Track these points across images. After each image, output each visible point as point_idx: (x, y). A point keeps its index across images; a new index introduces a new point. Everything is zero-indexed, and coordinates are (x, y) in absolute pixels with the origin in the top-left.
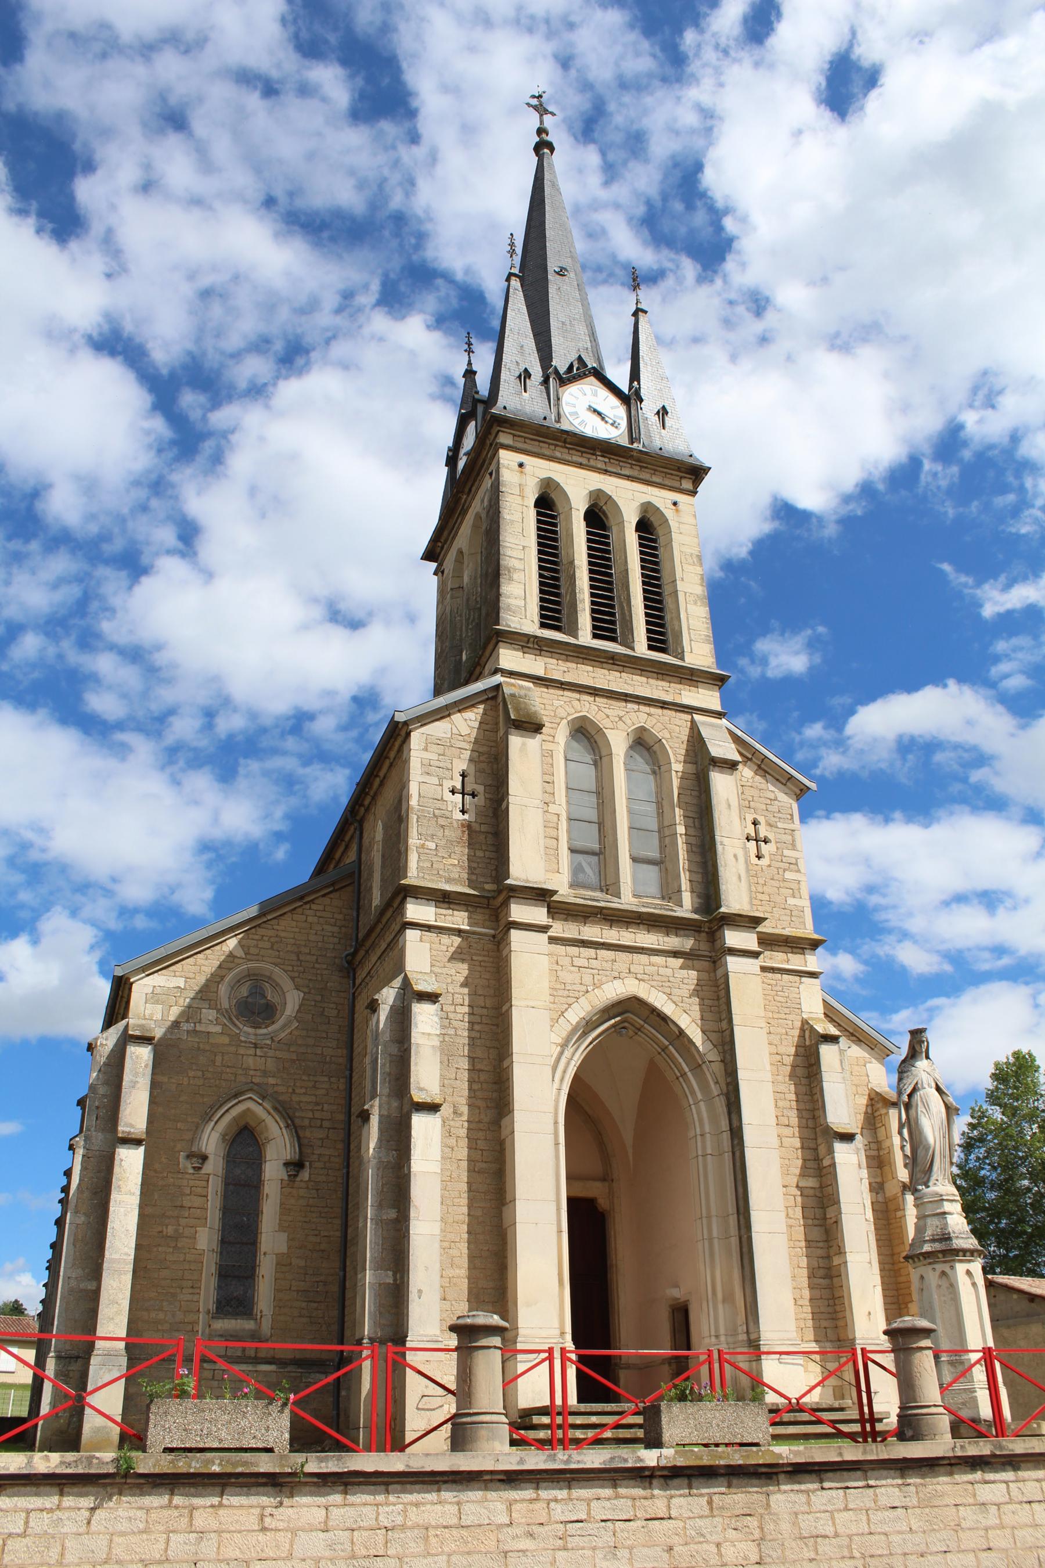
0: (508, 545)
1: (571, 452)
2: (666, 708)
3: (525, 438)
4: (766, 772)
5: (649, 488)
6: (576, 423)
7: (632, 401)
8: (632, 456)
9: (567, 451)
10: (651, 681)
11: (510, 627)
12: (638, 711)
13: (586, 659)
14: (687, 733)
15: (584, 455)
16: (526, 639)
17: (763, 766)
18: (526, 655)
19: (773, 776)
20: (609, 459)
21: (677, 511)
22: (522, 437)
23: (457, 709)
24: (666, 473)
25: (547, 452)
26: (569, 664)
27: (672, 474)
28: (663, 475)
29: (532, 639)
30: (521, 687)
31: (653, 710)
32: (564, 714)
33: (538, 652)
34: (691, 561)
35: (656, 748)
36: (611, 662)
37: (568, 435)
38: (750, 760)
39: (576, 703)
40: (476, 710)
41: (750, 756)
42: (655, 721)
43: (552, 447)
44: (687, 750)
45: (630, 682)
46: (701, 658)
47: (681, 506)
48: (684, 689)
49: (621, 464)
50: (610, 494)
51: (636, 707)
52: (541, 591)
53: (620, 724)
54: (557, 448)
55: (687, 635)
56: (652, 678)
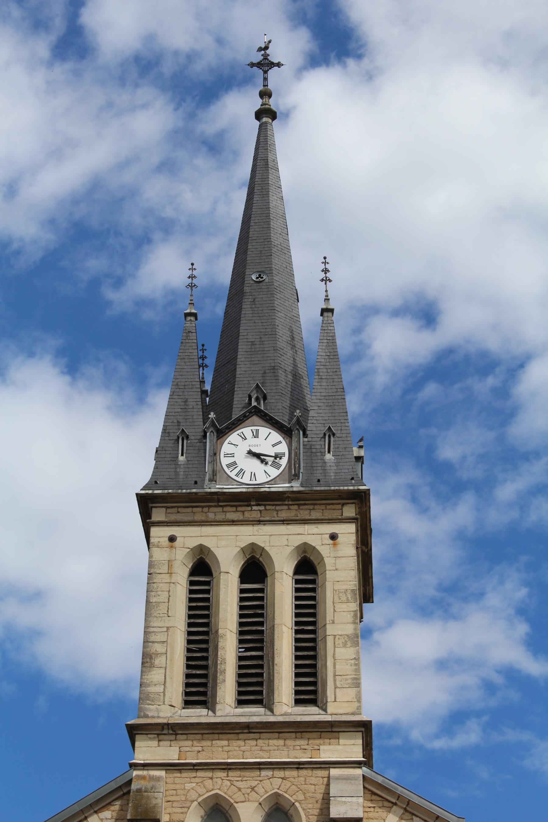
0: (152, 630)
1: (225, 509)
2: (302, 768)
3: (178, 507)
4: (413, 814)
5: (306, 526)
6: (232, 475)
7: (295, 433)
8: (288, 497)
9: (220, 509)
10: (289, 742)
11: (147, 716)
12: (273, 777)
13: (221, 733)
14: (322, 791)
15: (239, 509)
16: (160, 727)
17: (408, 808)
18: (161, 743)
19: (420, 818)
20: (265, 505)
21: (335, 544)
22: (172, 507)
23: (92, 811)
24: (326, 504)
25: (198, 517)
26: (204, 743)
27: (333, 504)
28: (323, 507)
29: (165, 727)
30: (152, 778)
31: (288, 773)
32: (193, 795)
33: (173, 737)
34: (344, 598)
35: (291, 812)
36: (246, 731)
37: (218, 495)
38: (395, 804)
39: (208, 783)
40: (112, 808)
41: (394, 801)
42: (289, 784)
43: (206, 510)
44: (321, 809)
45: (266, 748)
46: (345, 705)
47: (340, 539)
48: (324, 744)
49: (278, 508)
50: (262, 545)
51: (269, 773)
52: (188, 667)
53: (253, 794)
54: (212, 509)
55: (332, 683)
56: (290, 739)
